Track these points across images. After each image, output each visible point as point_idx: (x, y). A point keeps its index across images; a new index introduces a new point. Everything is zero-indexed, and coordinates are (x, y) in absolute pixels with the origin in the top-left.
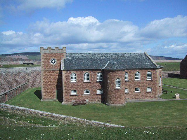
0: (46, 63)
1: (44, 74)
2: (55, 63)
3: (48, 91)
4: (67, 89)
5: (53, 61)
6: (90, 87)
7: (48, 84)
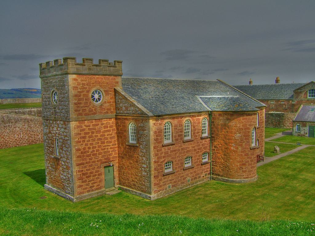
0: (82, 99)
1: (76, 131)
2: (99, 99)
3: (87, 173)
5: (96, 96)
7: (88, 156)
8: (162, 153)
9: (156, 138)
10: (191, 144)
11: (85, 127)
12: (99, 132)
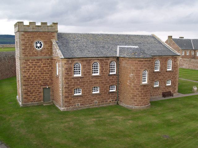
3: (31, 91)
4: (68, 88)
6: (100, 83)
7: (31, 81)
8: (72, 83)
9: (66, 72)
10: (99, 79)
11: (29, 63)
12: (40, 67)
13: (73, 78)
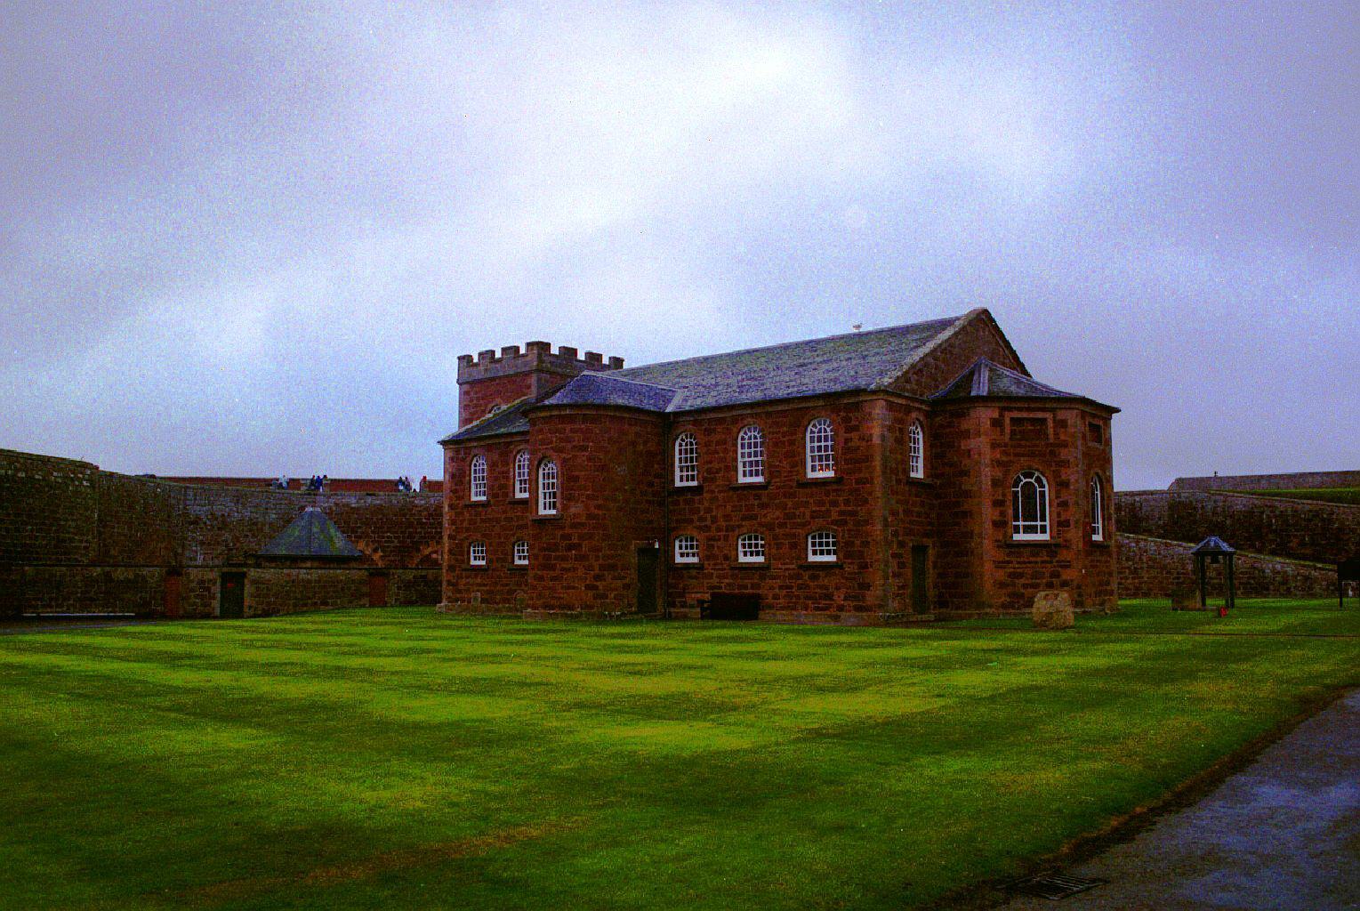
13: (470, 506)
